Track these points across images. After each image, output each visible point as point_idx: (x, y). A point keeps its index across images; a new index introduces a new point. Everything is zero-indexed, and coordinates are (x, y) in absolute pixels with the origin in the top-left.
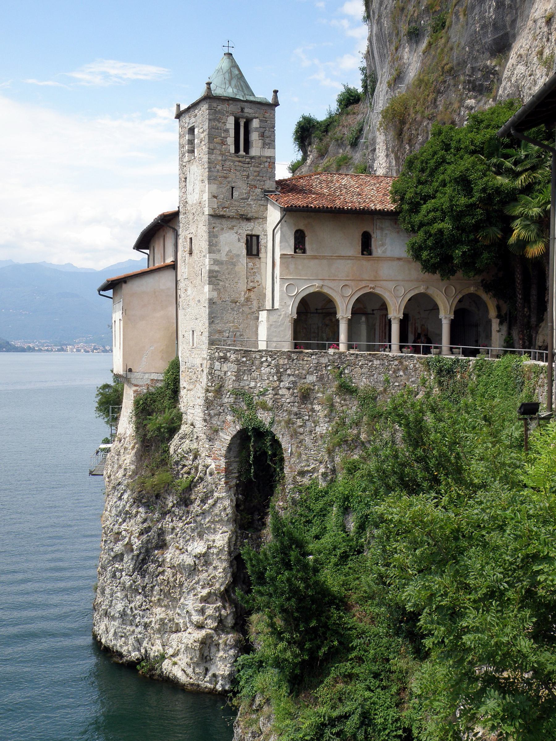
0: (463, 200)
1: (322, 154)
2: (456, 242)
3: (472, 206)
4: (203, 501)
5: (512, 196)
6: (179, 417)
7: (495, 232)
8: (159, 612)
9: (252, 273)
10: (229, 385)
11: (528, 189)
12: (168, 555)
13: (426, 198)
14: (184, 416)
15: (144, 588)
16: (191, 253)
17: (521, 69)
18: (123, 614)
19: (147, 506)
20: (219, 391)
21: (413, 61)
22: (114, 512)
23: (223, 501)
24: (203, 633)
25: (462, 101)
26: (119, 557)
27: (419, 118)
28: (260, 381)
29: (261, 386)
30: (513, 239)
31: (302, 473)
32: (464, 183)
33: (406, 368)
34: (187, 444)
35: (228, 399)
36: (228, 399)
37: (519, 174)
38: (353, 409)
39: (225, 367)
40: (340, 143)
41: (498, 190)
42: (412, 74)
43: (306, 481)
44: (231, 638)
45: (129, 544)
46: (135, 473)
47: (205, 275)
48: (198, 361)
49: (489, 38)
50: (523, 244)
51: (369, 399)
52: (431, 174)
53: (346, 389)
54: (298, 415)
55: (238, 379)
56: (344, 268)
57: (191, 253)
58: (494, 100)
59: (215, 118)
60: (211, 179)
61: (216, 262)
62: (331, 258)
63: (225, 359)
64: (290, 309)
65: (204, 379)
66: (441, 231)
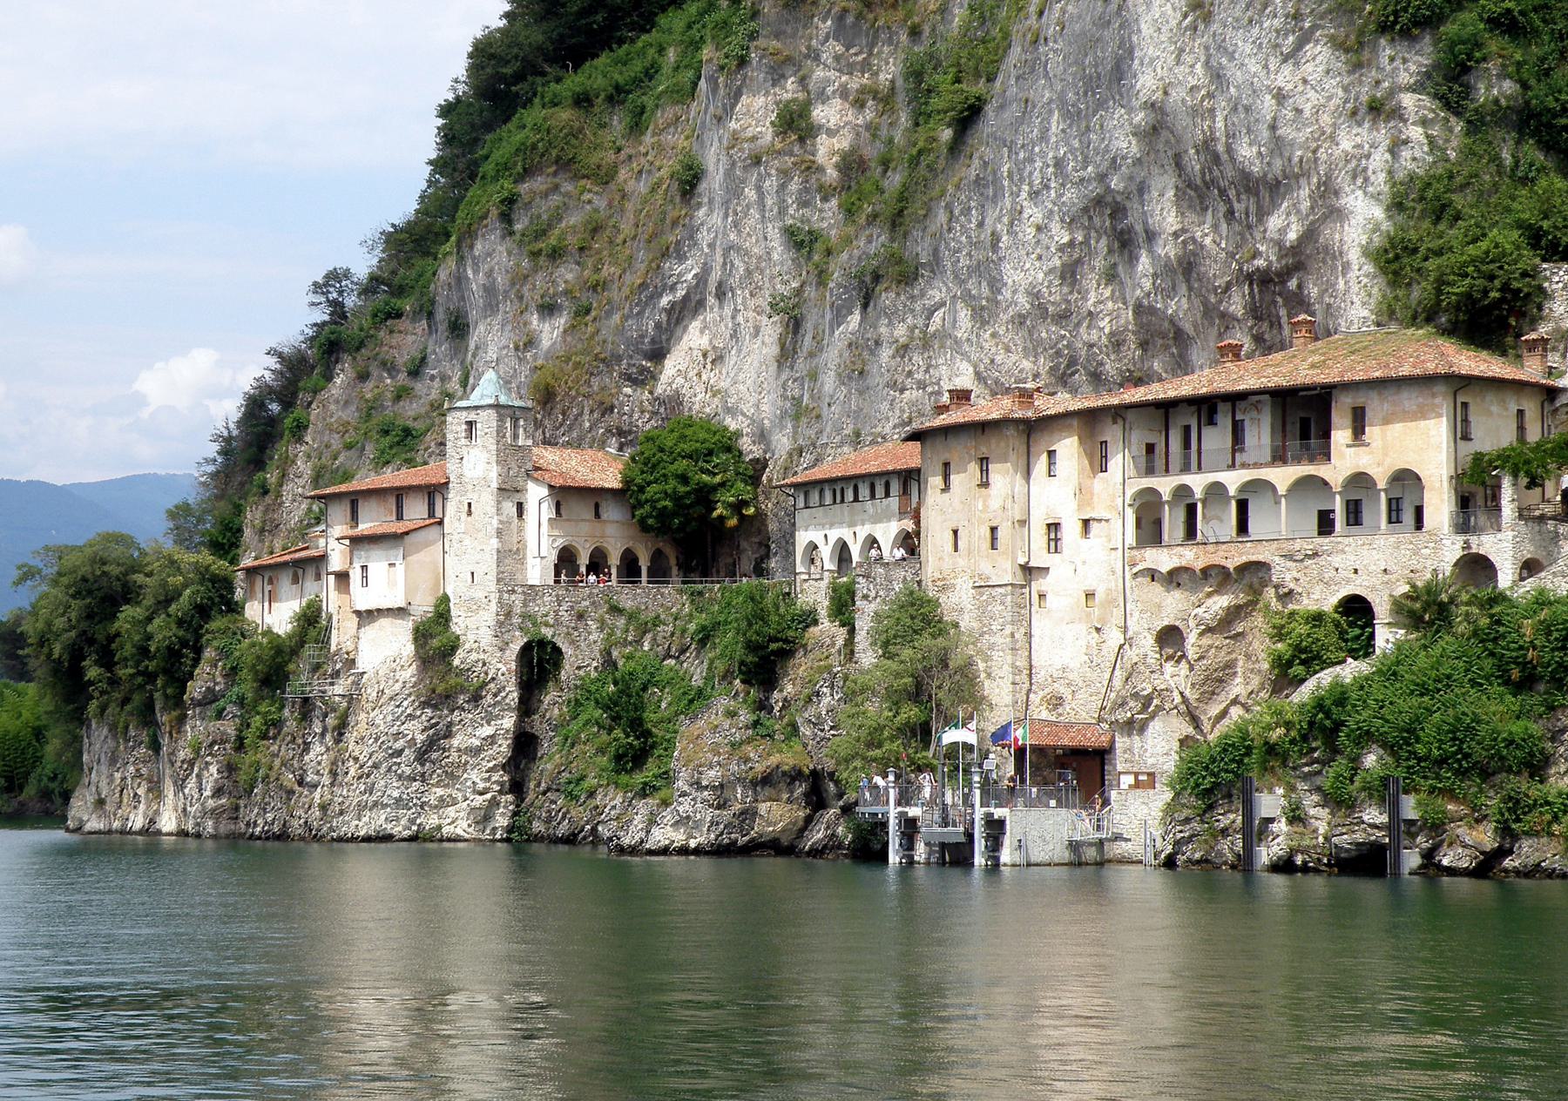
0: (682, 489)
1: (363, 377)
2: (675, 514)
3: (688, 493)
4: (495, 695)
5: (714, 488)
6: (458, 638)
7: (700, 510)
8: (440, 792)
9: (520, 530)
10: (518, 610)
11: (722, 484)
12: (455, 742)
13: (649, 484)
14: (462, 638)
15: (423, 775)
16: (470, 513)
17: (680, 380)
18: (398, 800)
19: (435, 707)
20: (508, 615)
21: (550, 333)
22: (390, 718)
23: (513, 695)
24: (489, 796)
25: (619, 388)
26: (399, 753)
27: (573, 393)
28: (543, 607)
29: (544, 610)
30: (715, 514)
31: (579, 668)
32: (684, 479)
33: (662, 595)
34: (474, 656)
35: (516, 620)
36: (516, 620)
37: (715, 474)
38: (621, 622)
39: (513, 597)
40: (389, 367)
41: (706, 485)
42: (546, 343)
43: (582, 673)
44: (510, 797)
45: (413, 739)
46: (421, 680)
47: (494, 533)
48: (480, 595)
49: (646, 347)
50: (721, 517)
51: (631, 617)
52: (654, 466)
53: (615, 610)
54: (575, 629)
55: (525, 605)
56: (585, 528)
57: (470, 513)
58: (651, 393)
59: (501, 419)
60: (498, 462)
61: (501, 522)
62: (577, 521)
63: (514, 591)
64: (553, 557)
65: (493, 607)
66: (665, 507)
